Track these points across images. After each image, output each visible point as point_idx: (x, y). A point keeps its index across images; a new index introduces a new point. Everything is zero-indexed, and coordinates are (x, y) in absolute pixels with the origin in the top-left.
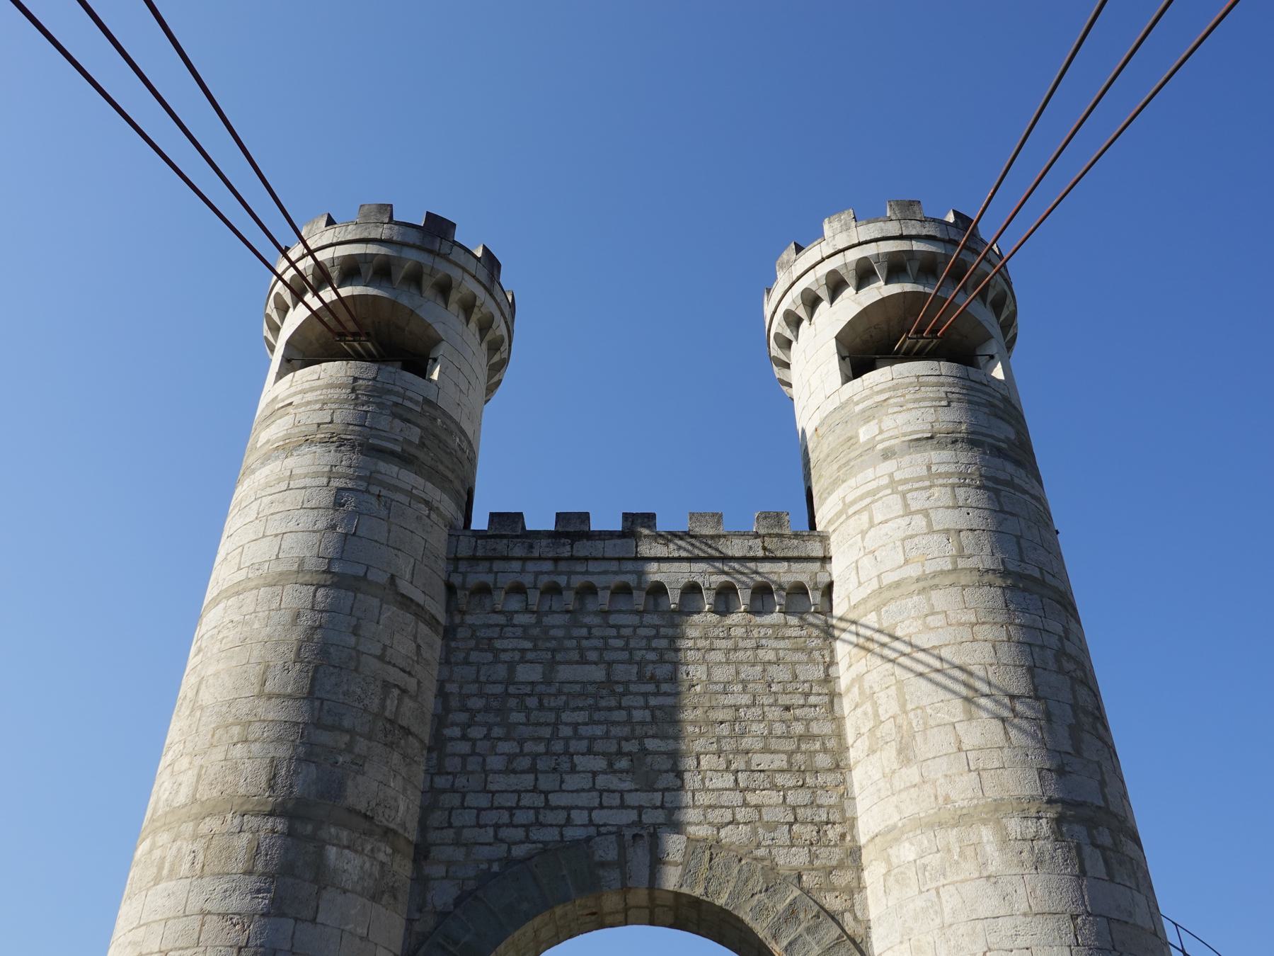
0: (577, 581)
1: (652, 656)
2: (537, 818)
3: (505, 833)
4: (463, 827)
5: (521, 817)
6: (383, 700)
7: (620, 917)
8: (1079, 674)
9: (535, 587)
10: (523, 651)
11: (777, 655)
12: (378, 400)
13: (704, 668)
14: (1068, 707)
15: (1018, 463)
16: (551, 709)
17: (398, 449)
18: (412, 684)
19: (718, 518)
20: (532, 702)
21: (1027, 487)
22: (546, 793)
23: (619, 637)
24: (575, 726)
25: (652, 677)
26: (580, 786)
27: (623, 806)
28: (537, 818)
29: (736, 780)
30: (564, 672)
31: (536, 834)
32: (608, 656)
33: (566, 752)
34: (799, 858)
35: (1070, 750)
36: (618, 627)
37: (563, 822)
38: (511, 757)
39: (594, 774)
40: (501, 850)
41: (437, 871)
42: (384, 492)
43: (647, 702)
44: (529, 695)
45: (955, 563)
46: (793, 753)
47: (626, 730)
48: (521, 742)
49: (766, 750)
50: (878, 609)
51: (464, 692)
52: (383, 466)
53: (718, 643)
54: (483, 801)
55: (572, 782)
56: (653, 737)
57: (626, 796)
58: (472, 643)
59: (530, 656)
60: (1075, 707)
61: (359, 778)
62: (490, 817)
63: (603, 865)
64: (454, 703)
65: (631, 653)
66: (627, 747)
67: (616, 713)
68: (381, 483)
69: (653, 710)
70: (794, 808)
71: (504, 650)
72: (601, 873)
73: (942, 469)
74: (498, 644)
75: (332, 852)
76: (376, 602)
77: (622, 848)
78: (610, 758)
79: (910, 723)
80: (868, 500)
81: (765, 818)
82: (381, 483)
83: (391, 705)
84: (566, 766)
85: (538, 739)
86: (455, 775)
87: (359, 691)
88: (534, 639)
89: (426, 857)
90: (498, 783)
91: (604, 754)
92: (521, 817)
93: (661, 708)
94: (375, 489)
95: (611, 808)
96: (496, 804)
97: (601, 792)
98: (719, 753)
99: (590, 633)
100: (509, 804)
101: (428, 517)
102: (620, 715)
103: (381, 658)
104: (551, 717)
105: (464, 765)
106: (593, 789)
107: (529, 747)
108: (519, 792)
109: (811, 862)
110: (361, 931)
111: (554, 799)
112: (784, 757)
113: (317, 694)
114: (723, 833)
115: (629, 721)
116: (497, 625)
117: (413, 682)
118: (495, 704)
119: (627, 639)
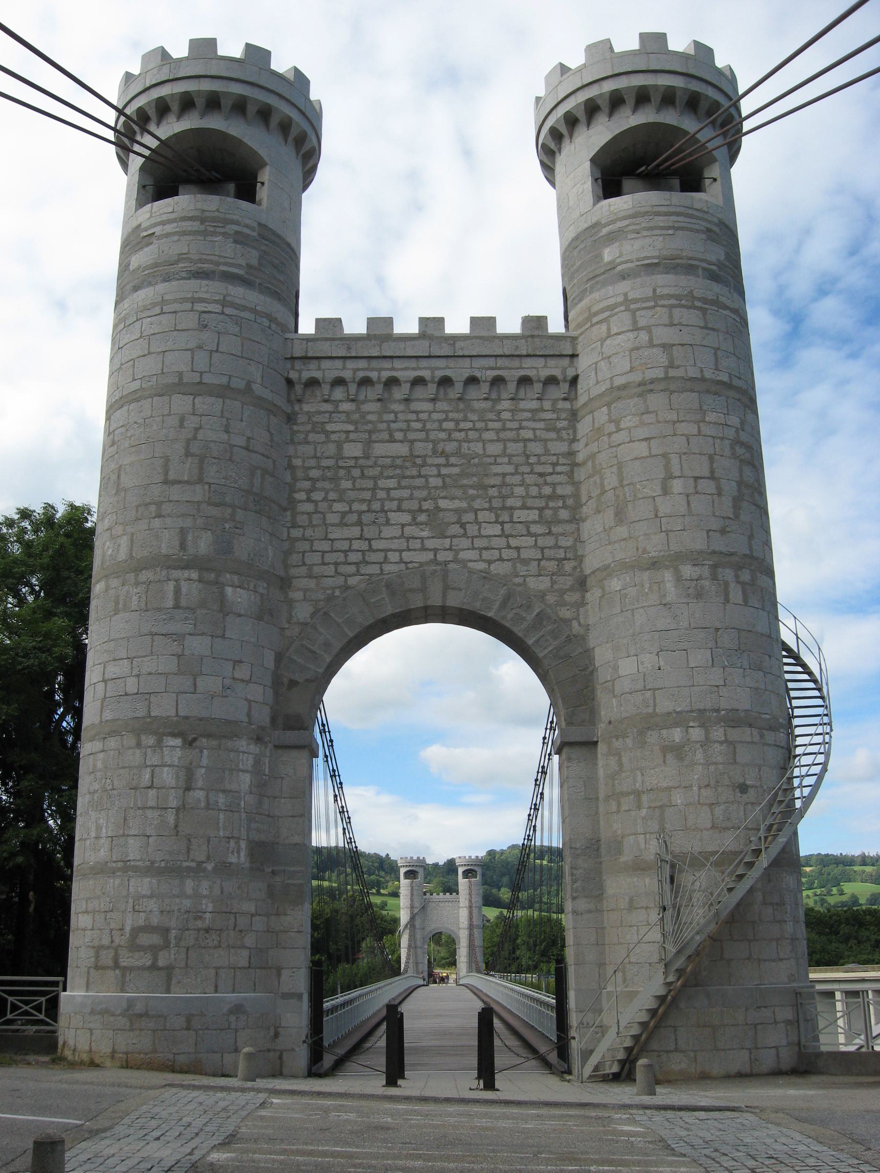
0: (386, 375)
1: (443, 435)
2: (364, 558)
3: (342, 569)
4: (314, 565)
8: (748, 456)
9: (354, 382)
10: (348, 432)
11: (534, 434)
12: (222, 230)
13: (480, 445)
14: (734, 484)
16: (370, 478)
17: (241, 272)
20: (356, 473)
21: (728, 303)
22: (369, 540)
23: (418, 420)
24: (388, 490)
25: (442, 453)
27: (424, 549)
28: (364, 558)
29: (502, 529)
30: (379, 449)
32: (411, 436)
33: (383, 510)
34: (544, 583)
35: (732, 516)
36: (417, 412)
37: (382, 560)
38: (344, 514)
39: (403, 526)
40: (340, 581)
41: (297, 595)
43: (439, 471)
44: (354, 467)
45: (666, 373)
47: (424, 493)
48: (350, 503)
49: (524, 507)
50: (608, 405)
51: (306, 465)
53: (491, 425)
54: (325, 546)
55: (387, 532)
56: (444, 498)
59: (352, 436)
62: (330, 558)
64: (300, 474)
65: (427, 433)
66: (426, 505)
71: (333, 432)
73: (666, 291)
74: (329, 427)
75: (229, 590)
76: (238, 404)
77: (424, 578)
78: (414, 513)
79: (625, 495)
80: (607, 314)
81: (522, 556)
84: (382, 520)
85: (363, 501)
86: (304, 528)
89: (289, 587)
91: (409, 511)
92: (353, 557)
93: (449, 476)
94: (228, 311)
95: (415, 550)
96: (335, 548)
97: (408, 539)
98: (490, 509)
99: (396, 417)
100: (343, 549)
101: (270, 328)
102: (419, 482)
103: (247, 448)
105: (310, 522)
107: (356, 506)
108: (350, 540)
109: (552, 586)
111: (376, 545)
112: (537, 512)
113: (206, 480)
114: (492, 567)
115: (426, 486)
116: (326, 412)
119: (424, 422)
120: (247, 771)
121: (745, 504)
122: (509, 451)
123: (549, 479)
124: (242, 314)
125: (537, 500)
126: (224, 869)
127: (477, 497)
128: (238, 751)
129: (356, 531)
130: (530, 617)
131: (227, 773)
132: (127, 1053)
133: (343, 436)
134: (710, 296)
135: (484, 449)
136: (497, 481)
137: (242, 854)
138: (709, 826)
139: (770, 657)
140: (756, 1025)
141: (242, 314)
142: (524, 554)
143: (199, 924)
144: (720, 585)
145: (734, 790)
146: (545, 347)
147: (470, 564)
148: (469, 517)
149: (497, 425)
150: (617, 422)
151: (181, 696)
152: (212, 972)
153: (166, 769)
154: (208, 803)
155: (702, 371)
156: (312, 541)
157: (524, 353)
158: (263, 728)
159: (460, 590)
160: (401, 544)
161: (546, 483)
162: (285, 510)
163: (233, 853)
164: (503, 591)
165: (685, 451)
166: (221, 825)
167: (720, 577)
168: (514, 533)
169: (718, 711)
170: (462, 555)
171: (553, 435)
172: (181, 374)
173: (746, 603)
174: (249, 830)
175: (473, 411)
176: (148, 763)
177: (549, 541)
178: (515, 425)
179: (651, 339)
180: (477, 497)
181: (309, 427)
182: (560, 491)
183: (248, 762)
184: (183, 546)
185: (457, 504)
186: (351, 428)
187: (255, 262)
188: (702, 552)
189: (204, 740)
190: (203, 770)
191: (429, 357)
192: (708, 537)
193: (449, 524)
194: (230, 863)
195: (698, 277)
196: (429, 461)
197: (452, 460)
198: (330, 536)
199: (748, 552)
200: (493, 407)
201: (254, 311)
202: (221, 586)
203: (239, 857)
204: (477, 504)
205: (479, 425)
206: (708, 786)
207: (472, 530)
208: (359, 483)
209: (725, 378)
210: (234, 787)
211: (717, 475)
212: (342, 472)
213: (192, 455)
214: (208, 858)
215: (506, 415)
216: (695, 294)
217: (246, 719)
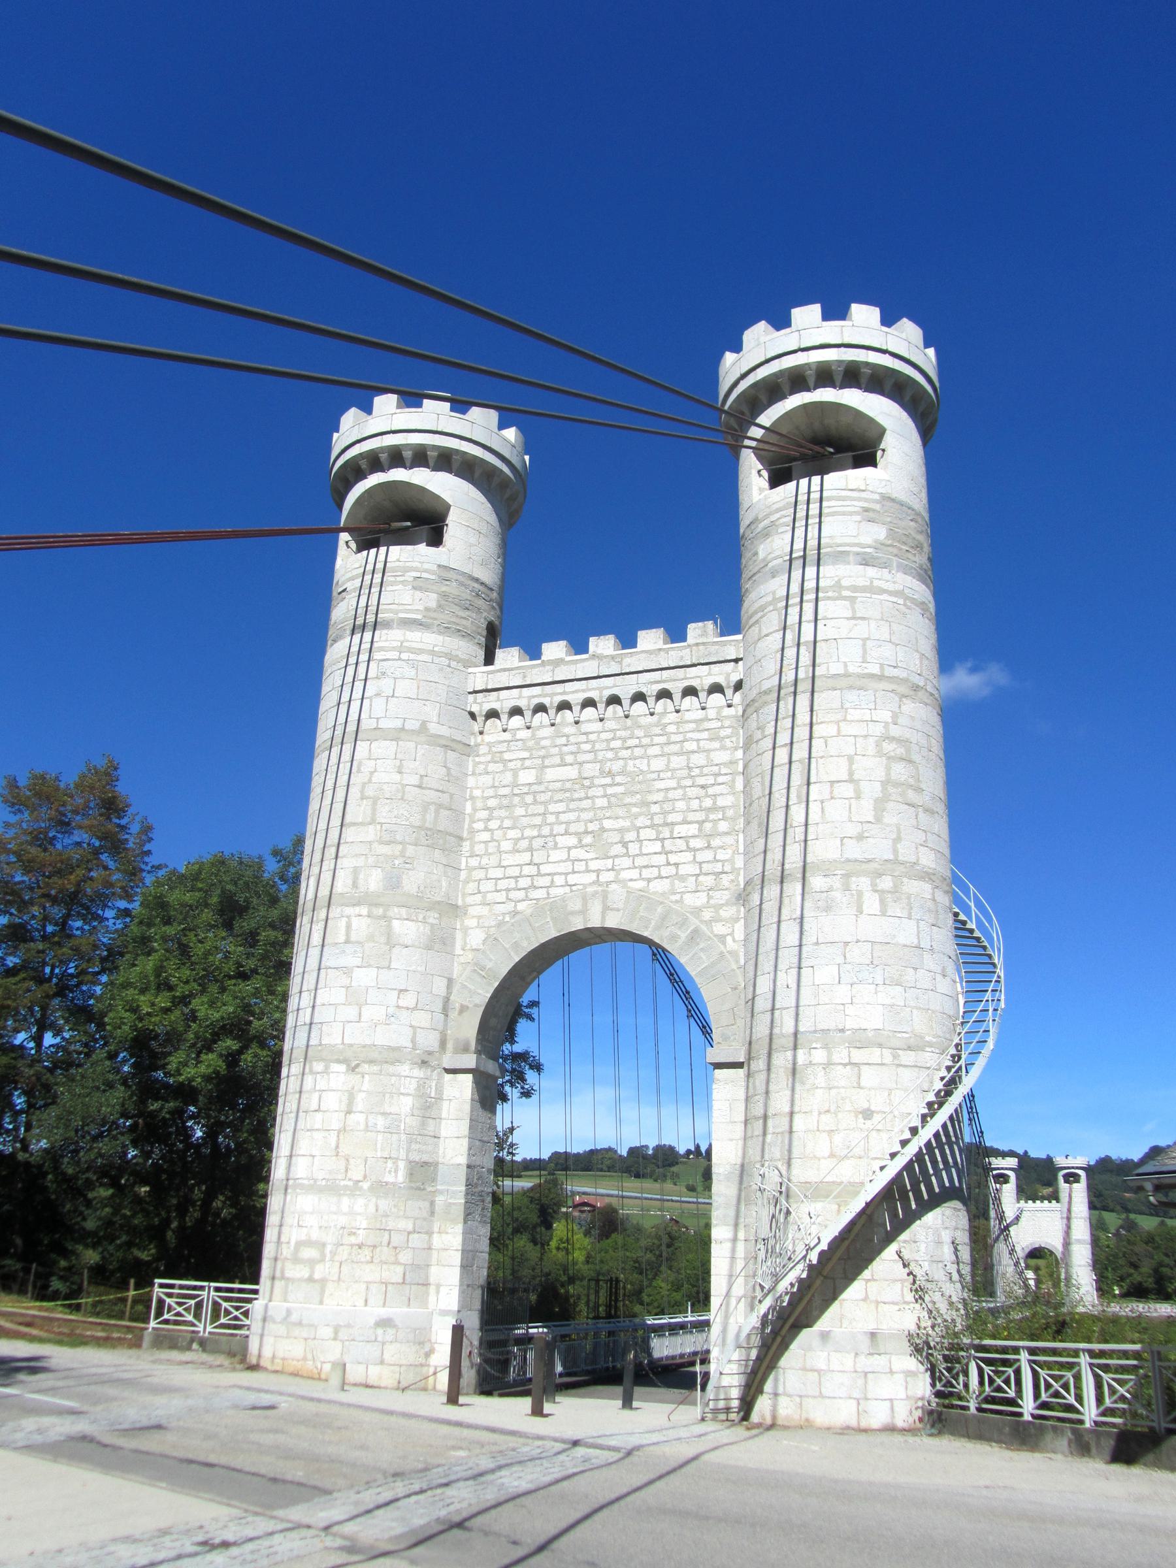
1: (610, 755)
3: (512, 895)
13: (646, 761)
17: (419, 617)
20: (529, 799)
26: (560, 858)
27: (588, 871)
30: (551, 774)
34: (700, 899)
39: (569, 849)
40: (510, 907)
46: (703, 822)
47: (590, 815)
49: (685, 822)
53: (657, 740)
54: (498, 873)
55: (556, 855)
57: (590, 863)
60: (885, 783)
61: (410, 873)
62: (503, 884)
63: (572, 913)
66: (591, 827)
67: (585, 802)
70: (700, 863)
72: (571, 918)
74: (507, 756)
76: (412, 745)
77: (585, 899)
81: (681, 872)
84: (551, 844)
87: (405, 813)
90: (508, 860)
92: (524, 883)
93: (614, 795)
94: (404, 656)
97: (573, 861)
98: (652, 826)
102: (586, 804)
103: (419, 787)
104: (541, 809)
105: (487, 850)
106: (568, 859)
108: (521, 865)
117: (446, 796)
120: (408, 1095)
122: (672, 765)
123: (711, 791)
124: (420, 658)
125: (697, 814)
126: (380, 1188)
127: (640, 814)
128: (399, 1076)
129: (526, 857)
130: (683, 935)
131: (387, 1096)
132: (283, 1359)
133: (519, 763)
134: (861, 582)
135: (649, 765)
136: (659, 797)
138: (827, 1154)
139: (916, 969)
140: (866, 1374)
141: (420, 658)
142: (683, 870)
143: (353, 1240)
144: (852, 895)
145: (856, 1117)
146: (710, 654)
147: (630, 884)
148: (631, 836)
149: (663, 739)
151: (348, 1026)
152: (364, 1286)
155: (846, 665)
157: (689, 663)
158: (430, 1053)
159: (618, 910)
160: (568, 867)
161: (707, 796)
163: (390, 1172)
164: (660, 909)
165: (821, 754)
166: (379, 1146)
167: (853, 887)
168: (674, 849)
169: (842, 1031)
170: (625, 875)
171: (716, 745)
173: (883, 913)
174: (408, 1151)
177: (707, 855)
178: (680, 738)
180: (640, 814)
181: (489, 758)
182: (721, 802)
183: (412, 1086)
184: (355, 885)
185: (621, 823)
186: (526, 754)
187: (433, 604)
188: (835, 861)
189: (366, 1066)
190: (363, 1095)
192: (842, 845)
193: (612, 844)
194: (387, 1183)
195: (849, 563)
196: (597, 782)
197: (618, 779)
198: (504, 863)
199: (892, 857)
200: (659, 721)
201: (432, 653)
203: (396, 1177)
204: (642, 821)
205: (645, 741)
206: (828, 1111)
207: (634, 848)
208: (533, 809)
209: (875, 669)
210: (393, 1110)
211: (856, 777)
212: (516, 800)
213: (367, 798)
214: (365, 1177)
216: (844, 583)
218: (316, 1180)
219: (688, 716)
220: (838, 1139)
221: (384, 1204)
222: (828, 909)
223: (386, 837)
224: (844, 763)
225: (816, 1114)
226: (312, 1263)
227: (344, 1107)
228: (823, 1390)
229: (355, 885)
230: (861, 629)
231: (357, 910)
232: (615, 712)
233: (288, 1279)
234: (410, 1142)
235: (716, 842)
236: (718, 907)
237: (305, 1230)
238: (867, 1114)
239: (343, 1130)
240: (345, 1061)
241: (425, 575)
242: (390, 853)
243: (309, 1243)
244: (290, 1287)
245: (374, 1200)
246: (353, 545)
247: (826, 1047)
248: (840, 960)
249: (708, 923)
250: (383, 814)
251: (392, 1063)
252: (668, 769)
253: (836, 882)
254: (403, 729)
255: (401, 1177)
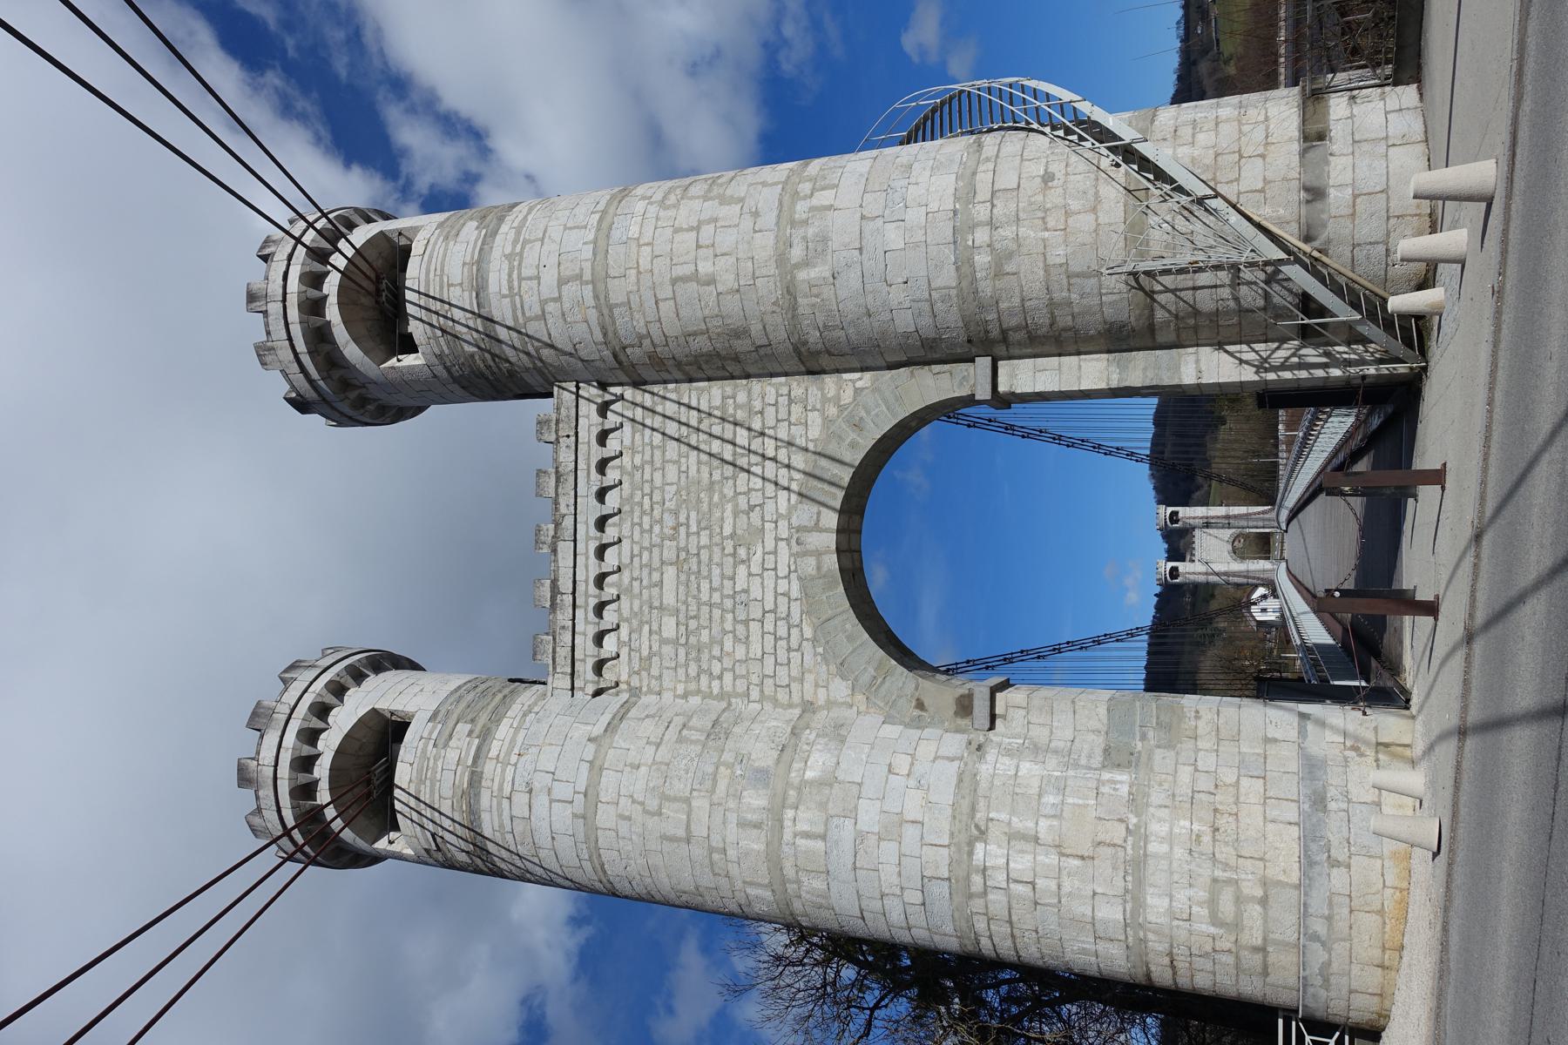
1: (657, 529)
3: (794, 644)
5: (782, 632)
6: (692, 742)
7: (856, 555)
8: (678, 191)
15: (501, 219)
18: (679, 721)
19: (540, 473)
20: (693, 624)
21: (521, 217)
22: (765, 612)
27: (775, 552)
30: (669, 599)
31: (795, 618)
32: (656, 563)
34: (815, 418)
38: (736, 639)
39: (750, 574)
40: (807, 646)
42: (516, 751)
45: (587, 283)
47: (716, 550)
48: (725, 632)
52: (493, 753)
53: (647, 476)
54: (769, 661)
55: (756, 592)
58: (644, 674)
59: (655, 627)
60: (706, 198)
62: (782, 656)
63: (819, 568)
64: (693, 686)
66: (729, 550)
68: (509, 754)
69: (700, 529)
72: (825, 569)
74: (645, 653)
75: (809, 775)
76: (611, 752)
77: (805, 554)
82: (509, 754)
83: (695, 736)
84: (744, 597)
88: (641, 623)
90: (756, 649)
91: (735, 566)
92: (782, 632)
93: (699, 523)
94: (514, 759)
102: (704, 555)
103: (658, 745)
104: (705, 609)
106: (761, 576)
108: (763, 633)
110: (867, 749)
111: (769, 606)
115: (709, 547)
118: (694, 654)
121: (729, 192)
122: (675, 458)
124: (519, 743)
126: (1137, 801)
127: (721, 492)
129: (754, 626)
131: (1017, 790)
132: (1384, 949)
137: (1118, 777)
141: (519, 743)
143: (1207, 839)
148: (742, 501)
150: (641, 337)
152: (1270, 826)
153: (1012, 865)
154: (1054, 816)
156: (765, 676)
159: (819, 513)
162: (730, 704)
167: (804, 216)
169: (955, 212)
170: (783, 510)
172: (575, 816)
174: (1090, 768)
175: (632, 496)
176: (1004, 885)
179: (554, 300)
180: (721, 492)
181: (644, 674)
183: (1006, 765)
184: (757, 826)
186: (646, 628)
189: (978, 815)
190: (1014, 819)
191: (575, 541)
196: (682, 544)
197: (682, 519)
198: (759, 655)
202: (804, 783)
203: (1121, 782)
204: (729, 492)
210: (1035, 783)
212: (693, 640)
213: (660, 807)
214: (1121, 820)
215: (638, 460)
216: (508, 250)
217: (956, 763)
218: (1127, 891)
219: (627, 442)
220: (1075, 205)
221: (1157, 797)
222: (824, 239)
223: (708, 784)
224: (679, 237)
225: (1047, 234)
226: (1239, 900)
227: (1029, 847)
228: (1378, 189)
229: (757, 826)
230: (555, 232)
231: (788, 823)
232: (614, 525)
233: (1265, 939)
234: (1077, 766)
235: (757, 405)
236: (825, 400)
237: (1195, 909)
238: (1048, 178)
239: (1060, 849)
240: (971, 844)
241: (434, 736)
242: (726, 781)
243: (1212, 903)
244: (1277, 936)
245: (1152, 810)
246: (393, 835)
247: (972, 228)
248: (880, 222)
249: (842, 409)
250: (679, 787)
251: (977, 783)
252: (677, 462)
253: (797, 236)
254: (591, 762)
255: (1123, 777)
